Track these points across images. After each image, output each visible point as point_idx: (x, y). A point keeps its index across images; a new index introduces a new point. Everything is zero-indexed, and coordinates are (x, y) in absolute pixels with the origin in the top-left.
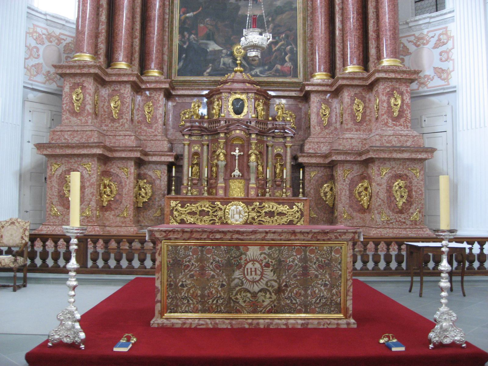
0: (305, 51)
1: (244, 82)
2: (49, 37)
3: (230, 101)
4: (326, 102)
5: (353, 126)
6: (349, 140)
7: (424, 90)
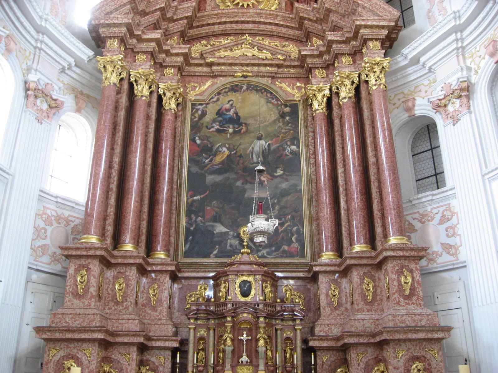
0: (311, 231)
1: (250, 264)
2: (59, 219)
3: (237, 283)
4: (335, 282)
5: (364, 306)
6: (361, 321)
7: (433, 267)
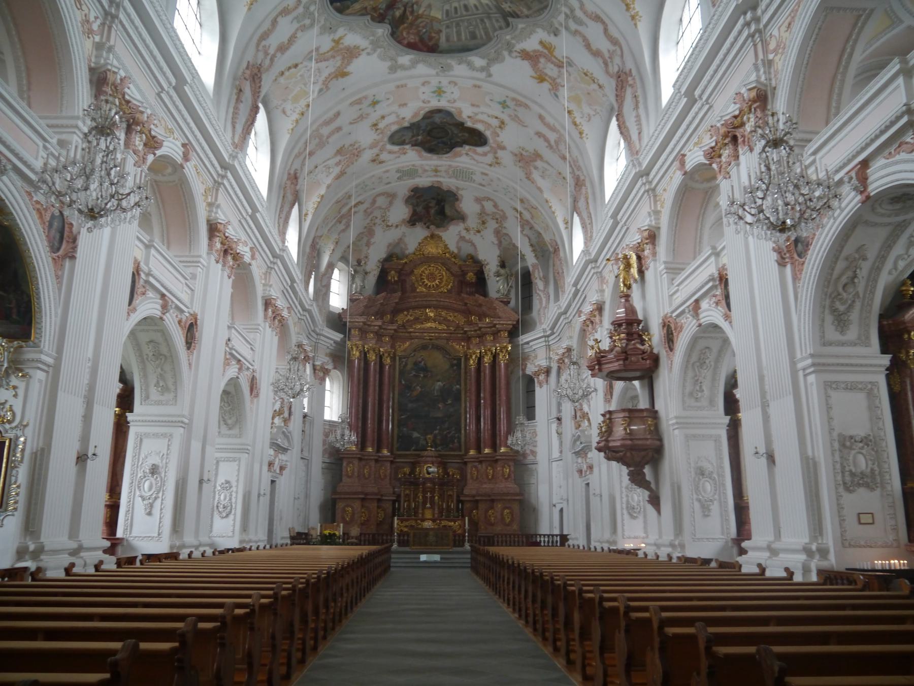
4: (476, 467)
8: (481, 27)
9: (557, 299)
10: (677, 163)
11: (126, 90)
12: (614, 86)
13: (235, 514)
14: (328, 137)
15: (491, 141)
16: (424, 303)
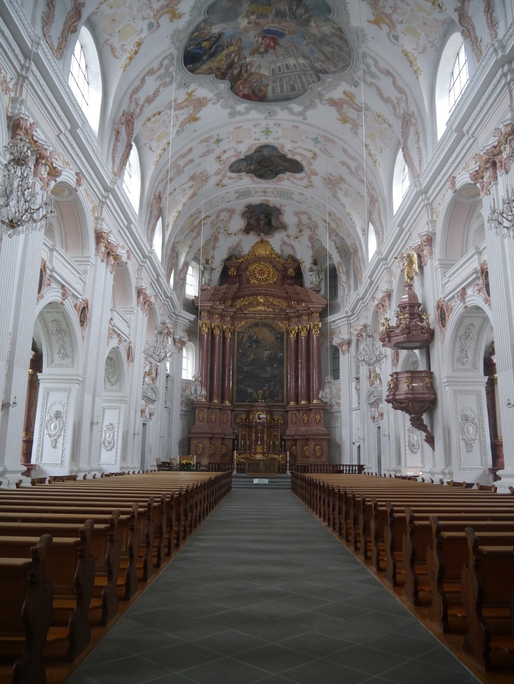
4: (295, 414)
7: (333, 411)
8: (298, 81)
9: (356, 288)
10: (449, 184)
11: (34, 133)
12: (401, 125)
13: (117, 448)
14: (184, 167)
15: (306, 169)
16: (256, 292)
